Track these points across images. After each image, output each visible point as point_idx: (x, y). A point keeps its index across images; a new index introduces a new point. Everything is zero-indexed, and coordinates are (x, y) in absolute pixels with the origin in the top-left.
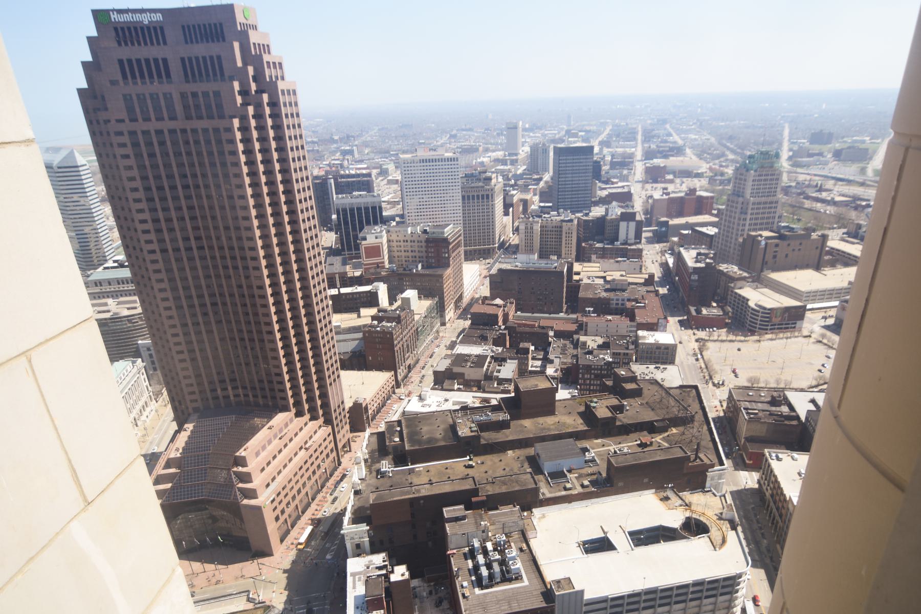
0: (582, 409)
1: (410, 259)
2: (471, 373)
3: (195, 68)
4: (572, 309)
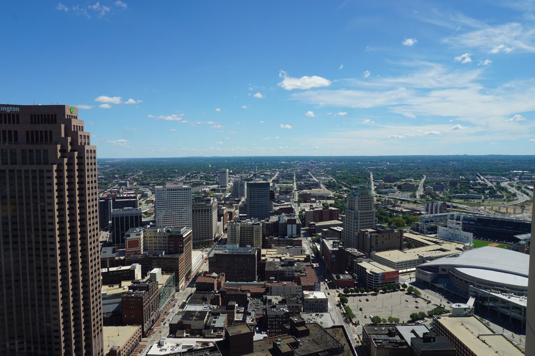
0: (271, 347)
1: (158, 248)
3: (35, 137)
4: (262, 279)
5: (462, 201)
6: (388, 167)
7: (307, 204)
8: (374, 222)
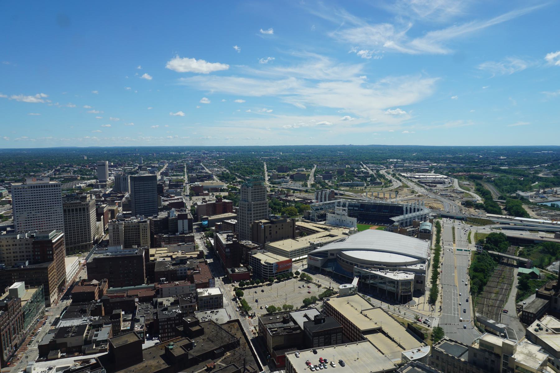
0: (163, 352)
1: (19, 258)
2: (71, 341)
4: (151, 281)
5: (348, 188)
6: (281, 157)
7: (200, 197)
8: (268, 213)
